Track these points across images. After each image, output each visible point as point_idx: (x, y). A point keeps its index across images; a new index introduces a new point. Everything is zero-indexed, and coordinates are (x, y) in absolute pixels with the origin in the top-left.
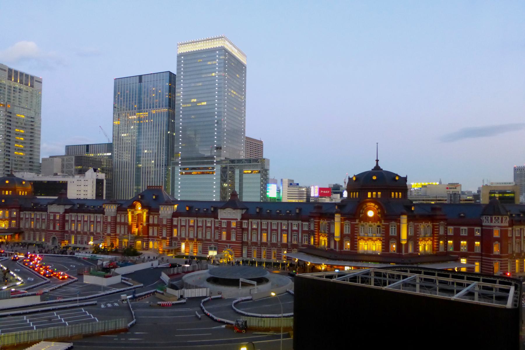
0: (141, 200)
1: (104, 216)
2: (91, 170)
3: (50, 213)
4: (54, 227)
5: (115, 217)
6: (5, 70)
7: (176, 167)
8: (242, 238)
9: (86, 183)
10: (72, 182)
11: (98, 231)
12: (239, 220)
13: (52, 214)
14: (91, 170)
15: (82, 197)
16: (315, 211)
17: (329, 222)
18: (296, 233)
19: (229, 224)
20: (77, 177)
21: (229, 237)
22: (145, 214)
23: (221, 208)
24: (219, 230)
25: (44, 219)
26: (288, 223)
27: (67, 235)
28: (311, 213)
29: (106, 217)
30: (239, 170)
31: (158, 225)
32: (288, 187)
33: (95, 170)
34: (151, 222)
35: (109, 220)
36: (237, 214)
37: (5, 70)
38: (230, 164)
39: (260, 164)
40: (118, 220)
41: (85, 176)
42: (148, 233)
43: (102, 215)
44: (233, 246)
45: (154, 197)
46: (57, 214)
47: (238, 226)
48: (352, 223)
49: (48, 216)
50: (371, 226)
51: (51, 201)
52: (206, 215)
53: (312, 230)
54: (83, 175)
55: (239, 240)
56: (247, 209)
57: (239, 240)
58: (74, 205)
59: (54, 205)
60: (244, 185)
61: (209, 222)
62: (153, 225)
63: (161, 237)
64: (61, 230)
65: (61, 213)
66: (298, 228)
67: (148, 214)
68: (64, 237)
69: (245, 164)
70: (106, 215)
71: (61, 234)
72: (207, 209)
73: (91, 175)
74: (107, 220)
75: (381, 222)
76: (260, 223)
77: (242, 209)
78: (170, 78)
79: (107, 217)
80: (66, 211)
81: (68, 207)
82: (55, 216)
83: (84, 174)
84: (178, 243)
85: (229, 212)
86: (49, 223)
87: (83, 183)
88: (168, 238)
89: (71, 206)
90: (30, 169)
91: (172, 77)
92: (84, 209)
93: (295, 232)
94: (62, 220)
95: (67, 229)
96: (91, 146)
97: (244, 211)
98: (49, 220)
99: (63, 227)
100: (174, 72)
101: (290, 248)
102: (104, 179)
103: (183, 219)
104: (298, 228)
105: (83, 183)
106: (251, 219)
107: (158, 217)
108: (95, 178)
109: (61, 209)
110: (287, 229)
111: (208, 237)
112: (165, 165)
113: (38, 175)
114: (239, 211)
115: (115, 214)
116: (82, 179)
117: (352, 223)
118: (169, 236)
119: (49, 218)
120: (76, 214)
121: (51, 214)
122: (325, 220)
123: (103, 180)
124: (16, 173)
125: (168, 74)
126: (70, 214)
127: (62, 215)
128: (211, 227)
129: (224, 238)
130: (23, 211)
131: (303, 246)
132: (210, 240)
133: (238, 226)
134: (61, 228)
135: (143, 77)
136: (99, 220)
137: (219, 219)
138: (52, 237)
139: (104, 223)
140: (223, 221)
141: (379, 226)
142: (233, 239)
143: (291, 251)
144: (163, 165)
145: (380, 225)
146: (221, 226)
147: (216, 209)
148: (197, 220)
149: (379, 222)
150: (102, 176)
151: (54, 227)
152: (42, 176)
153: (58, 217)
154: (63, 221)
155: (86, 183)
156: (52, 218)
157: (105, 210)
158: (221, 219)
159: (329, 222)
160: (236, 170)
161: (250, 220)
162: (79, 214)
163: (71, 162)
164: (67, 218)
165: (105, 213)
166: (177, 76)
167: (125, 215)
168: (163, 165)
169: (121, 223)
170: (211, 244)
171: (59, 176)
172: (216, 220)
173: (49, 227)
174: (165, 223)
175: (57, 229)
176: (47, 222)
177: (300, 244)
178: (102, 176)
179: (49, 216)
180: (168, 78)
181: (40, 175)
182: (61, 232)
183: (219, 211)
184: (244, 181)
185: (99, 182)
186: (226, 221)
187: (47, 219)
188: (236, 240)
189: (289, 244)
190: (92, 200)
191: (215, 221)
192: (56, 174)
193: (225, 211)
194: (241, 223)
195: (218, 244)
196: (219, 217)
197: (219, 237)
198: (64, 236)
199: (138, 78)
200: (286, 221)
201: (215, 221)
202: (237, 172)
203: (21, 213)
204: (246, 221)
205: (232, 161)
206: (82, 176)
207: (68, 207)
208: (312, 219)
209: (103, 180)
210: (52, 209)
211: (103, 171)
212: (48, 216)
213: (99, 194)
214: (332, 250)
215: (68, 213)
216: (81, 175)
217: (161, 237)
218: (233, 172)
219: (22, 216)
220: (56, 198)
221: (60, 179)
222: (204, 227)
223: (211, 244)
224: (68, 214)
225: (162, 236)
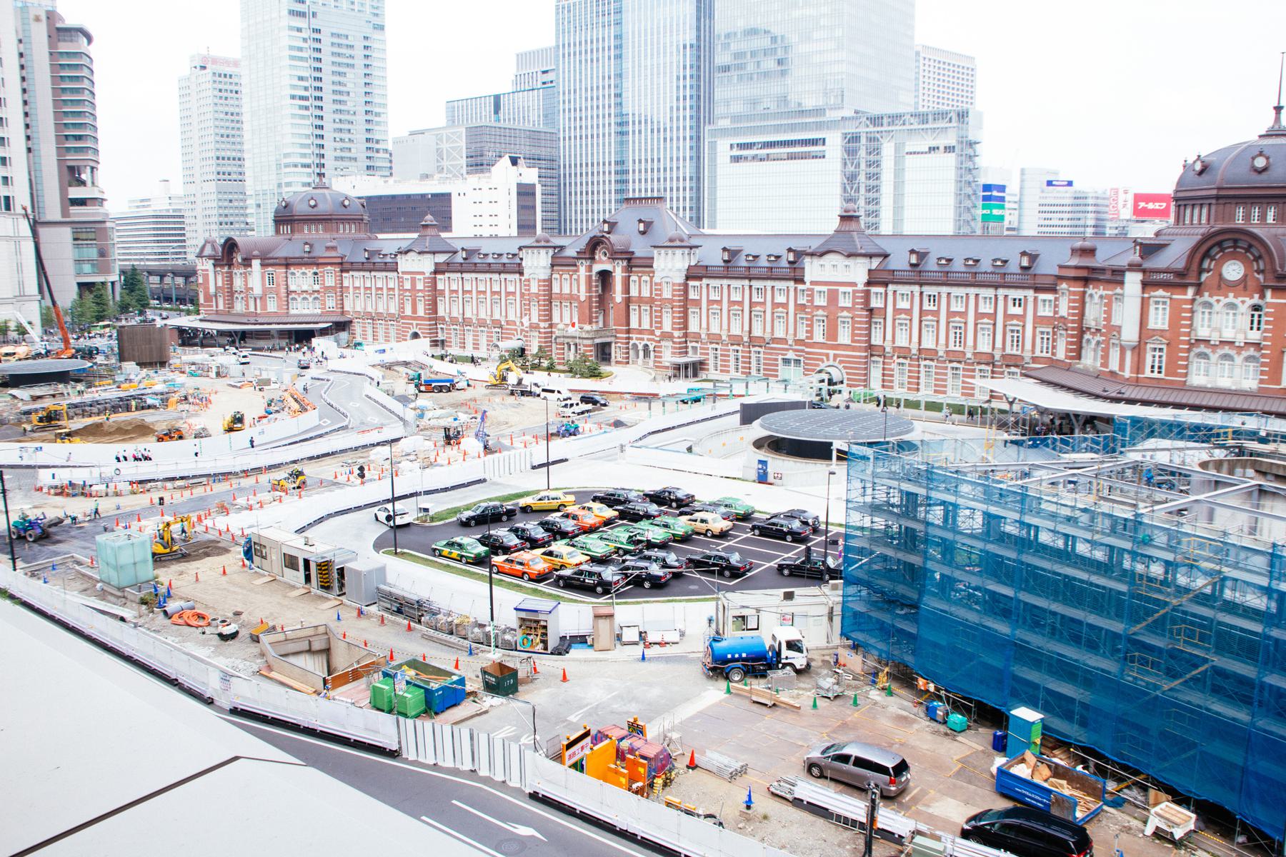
1: (523, 278)
5: (549, 282)
8: (869, 335)
11: (511, 317)
13: (409, 277)
19: (833, 297)
20: (474, 180)
21: (832, 333)
24: (807, 313)
31: (650, 301)
34: (634, 292)
36: (858, 272)
44: (843, 356)
55: (859, 341)
57: (859, 341)
62: (641, 300)
63: (658, 332)
83: (489, 171)
84: (701, 348)
103: (715, 283)
110: (992, 311)
111: (780, 333)
118: (680, 329)
129: (818, 337)
131: (1034, 359)
132: (784, 341)
133: (858, 303)
136: (511, 289)
138: (411, 332)
139: (522, 295)
140: (817, 288)
142: (844, 337)
146: (812, 301)
148: (751, 287)
153: (420, 286)
156: (408, 286)
158: (812, 283)
165: (526, 271)
170: (787, 350)
172: (800, 287)
174: (667, 294)
175: (421, 312)
177: (1027, 355)
185: (525, 192)
186: (825, 288)
188: (853, 341)
191: (796, 289)
195: (803, 351)
197: (807, 332)
203: (344, 275)
219: (346, 284)
223: (787, 350)
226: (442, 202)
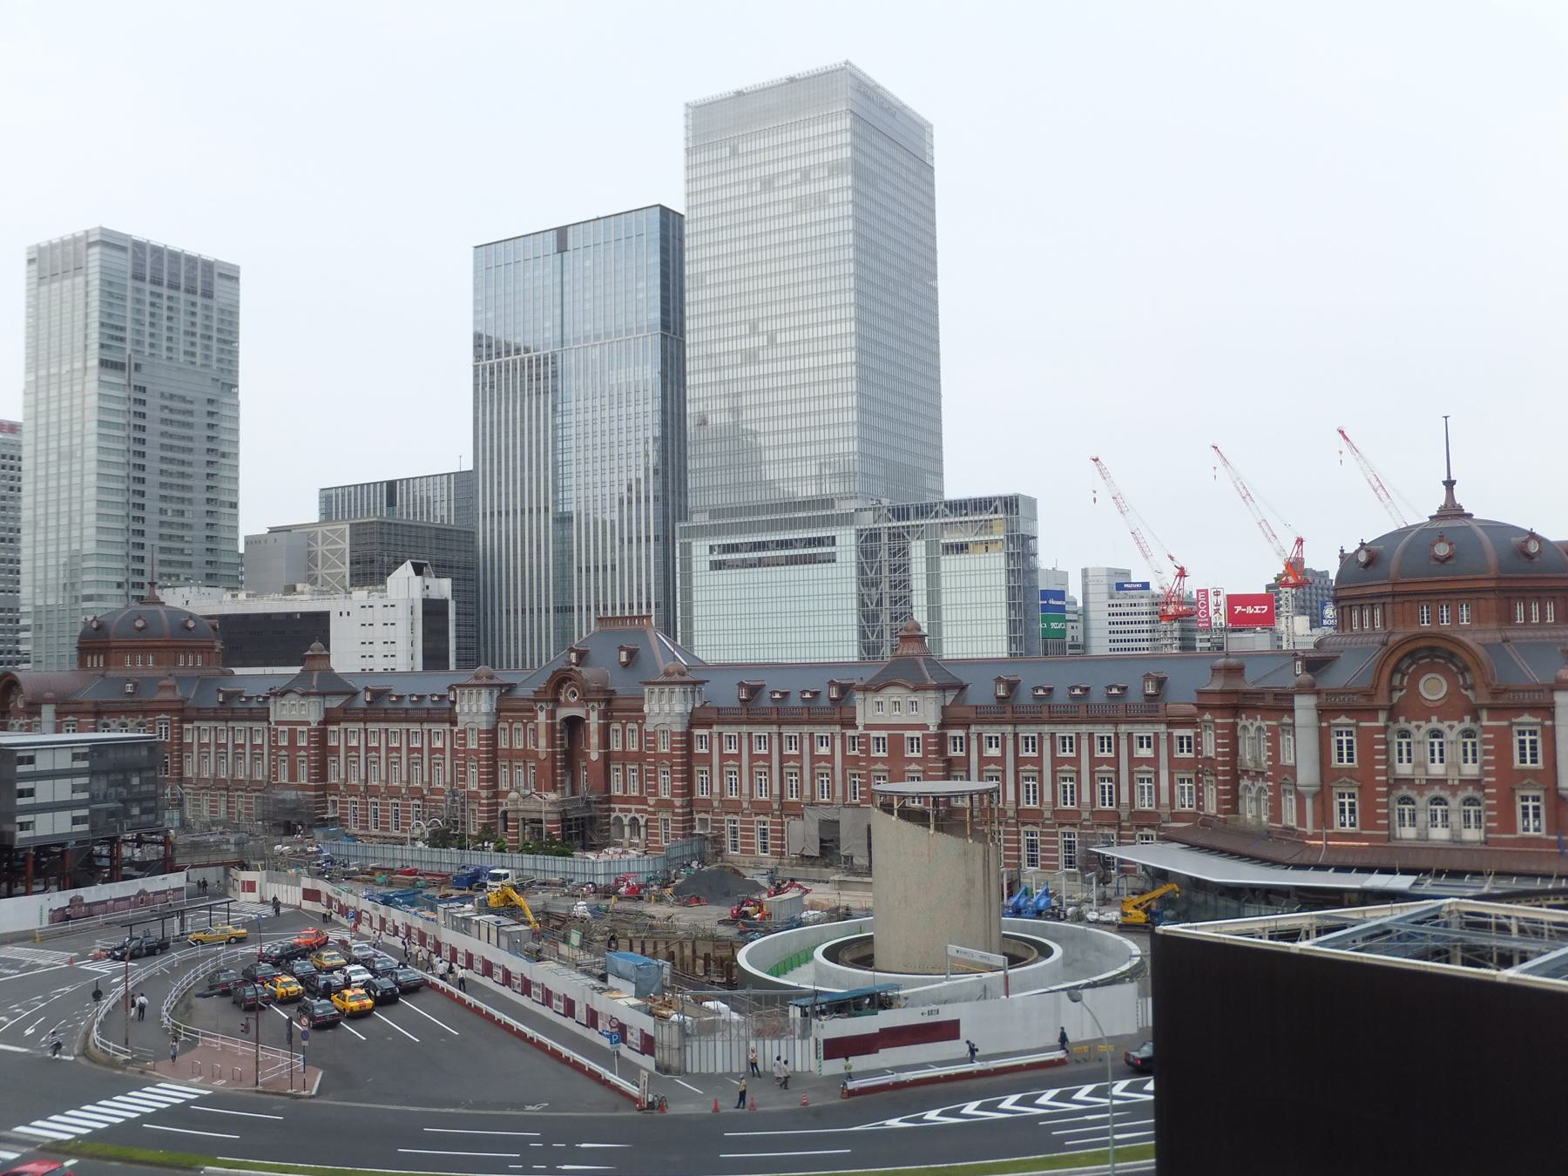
0: (578, 669)
1: (456, 729)
2: (406, 570)
3: (278, 723)
4: (293, 775)
6: (123, 249)
7: (694, 544)
9: (391, 615)
10: (345, 614)
12: (933, 729)
13: (285, 728)
14: (406, 570)
15: (379, 665)
16: (1217, 685)
17: (1274, 723)
18: (1149, 772)
20: (360, 595)
22: (594, 716)
23: (865, 689)
25: (261, 746)
26: (1116, 734)
27: (333, 798)
28: (1200, 693)
29: (460, 731)
30: (924, 543)
31: (640, 757)
32: (1112, 597)
33: (418, 569)
34: (616, 746)
35: (473, 745)
36: (927, 711)
37: (123, 249)
38: (890, 525)
39: (1002, 516)
40: (503, 744)
41: (384, 591)
42: (608, 788)
43: (447, 726)
45: (624, 657)
46: (300, 728)
47: (931, 752)
48: (1362, 724)
49: (274, 735)
50: (1436, 734)
51: (280, 685)
52: (810, 714)
53: (1210, 758)
54: (379, 587)
56: (962, 688)
58: (355, 694)
59: (288, 696)
60: (945, 599)
61: (828, 743)
62: (625, 757)
63: (651, 800)
64: (316, 781)
65: (314, 725)
66: (1157, 751)
67: (607, 715)
68: (326, 808)
69: (947, 520)
70: (460, 726)
71: (316, 796)
72: (815, 694)
73: (405, 585)
74: (465, 745)
75: (1476, 718)
76: (1010, 738)
77: (942, 688)
78: (664, 226)
79: (464, 732)
80: (329, 718)
81: (335, 703)
82: (293, 736)
83: (383, 582)
85: (895, 699)
86: (275, 760)
87: (378, 615)
88: (678, 802)
89: (345, 698)
90: (209, 576)
91: (670, 222)
92: (388, 705)
93: (1144, 768)
94: (315, 748)
95: (333, 780)
96: (401, 485)
97: (950, 697)
98: (274, 747)
99: (322, 771)
100: (678, 205)
101: (1130, 829)
102: (450, 598)
104: (1157, 751)
105: (378, 615)
106: (976, 723)
107: (640, 726)
108: (417, 596)
109: (310, 712)
112: (657, 539)
113: (233, 596)
114: (931, 694)
115: (492, 719)
116: (375, 599)
117: (1362, 724)
118: (683, 795)
119: (276, 741)
120: (361, 725)
121: (280, 728)
122: (1259, 717)
123: (445, 602)
124: (165, 590)
125: (656, 213)
126: (343, 725)
127: (315, 730)
128: (830, 759)
130: (191, 721)
131: (1176, 817)
133: (931, 752)
134: (315, 774)
135: (570, 230)
137: (860, 728)
139: (454, 752)
141: (1468, 733)
143: (1133, 837)
144: (648, 539)
145: (1473, 726)
146: (867, 751)
147: (845, 690)
149: (1467, 718)
150: (443, 588)
151: (293, 775)
152: (248, 596)
154: (323, 751)
155: (391, 615)
157: (457, 708)
158: (867, 727)
159: (1274, 723)
160: (913, 543)
161: (973, 729)
162: (372, 727)
163: (337, 543)
164: (332, 743)
165: (459, 718)
166: (686, 219)
167: (525, 725)
168: (648, 539)
169: (512, 754)
171: (302, 593)
172: (850, 733)
173: (276, 773)
176: (269, 755)
178: (443, 588)
179: (275, 736)
180: (657, 226)
181: (242, 596)
182: (316, 789)
183: (858, 696)
184: (945, 582)
185: (433, 611)
186: (884, 734)
187: (270, 745)
189: (1124, 815)
190: (412, 673)
191: (843, 735)
192: (291, 589)
193: (879, 699)
194: (942, 740)
196: (859, 721)
198: (326, 802)
199: (552, 237)
200: (1110, 727)
201: (843, 735)
202: (918, 549)
203: (186, 726)
204: (961, 733)
205: (900, 513)
206: (377, 591)
207: (335, 703)
208: (1207, 717)
209: (445, 602)
210: (286, 710)
211: (441, 570)
212: (274, 735)
213: (434, 658)
214: (1289, 830)
215: (337, 722)
216: (370, 588)
217: (651, 800)
218: (904, 551)
220: (296, 670)
221: (303, 602)
222: (807, 758)
224: (335, 728)
225: (655, 794)
226: (317, 625)
